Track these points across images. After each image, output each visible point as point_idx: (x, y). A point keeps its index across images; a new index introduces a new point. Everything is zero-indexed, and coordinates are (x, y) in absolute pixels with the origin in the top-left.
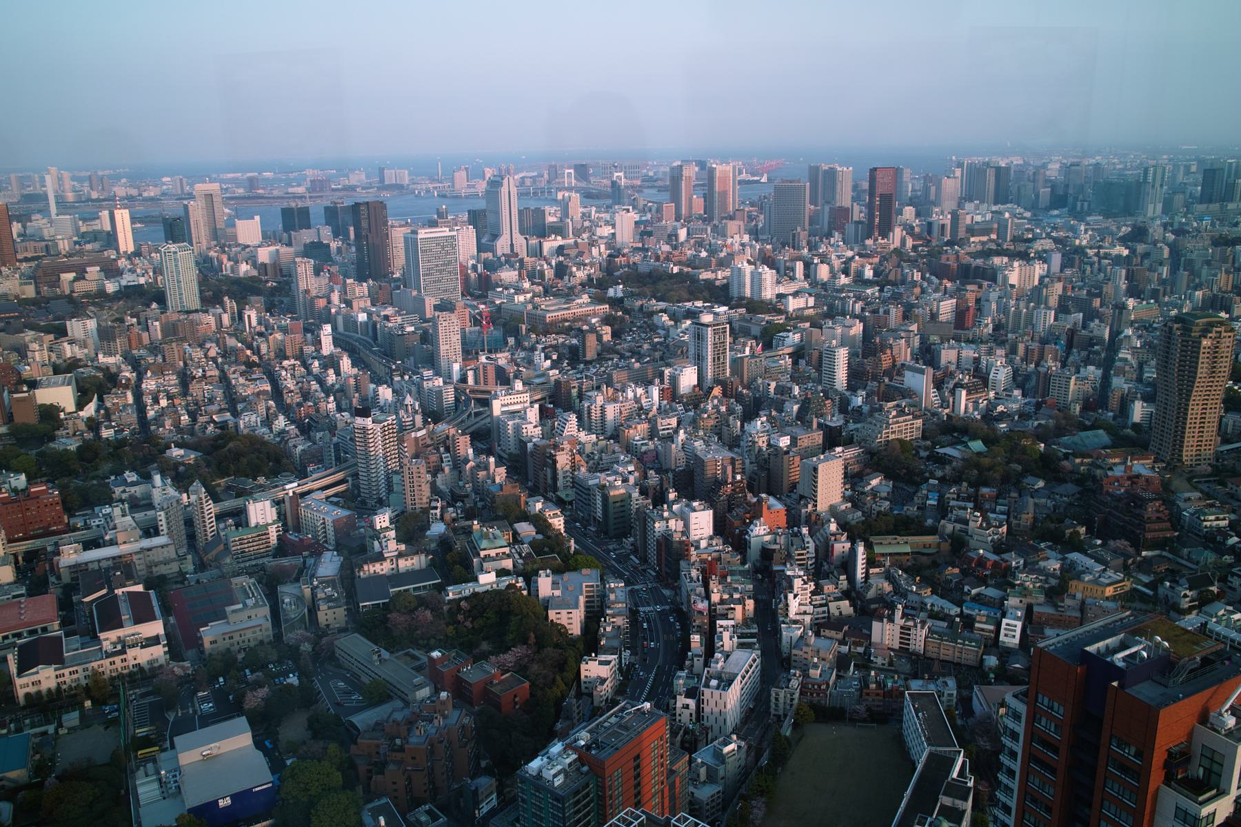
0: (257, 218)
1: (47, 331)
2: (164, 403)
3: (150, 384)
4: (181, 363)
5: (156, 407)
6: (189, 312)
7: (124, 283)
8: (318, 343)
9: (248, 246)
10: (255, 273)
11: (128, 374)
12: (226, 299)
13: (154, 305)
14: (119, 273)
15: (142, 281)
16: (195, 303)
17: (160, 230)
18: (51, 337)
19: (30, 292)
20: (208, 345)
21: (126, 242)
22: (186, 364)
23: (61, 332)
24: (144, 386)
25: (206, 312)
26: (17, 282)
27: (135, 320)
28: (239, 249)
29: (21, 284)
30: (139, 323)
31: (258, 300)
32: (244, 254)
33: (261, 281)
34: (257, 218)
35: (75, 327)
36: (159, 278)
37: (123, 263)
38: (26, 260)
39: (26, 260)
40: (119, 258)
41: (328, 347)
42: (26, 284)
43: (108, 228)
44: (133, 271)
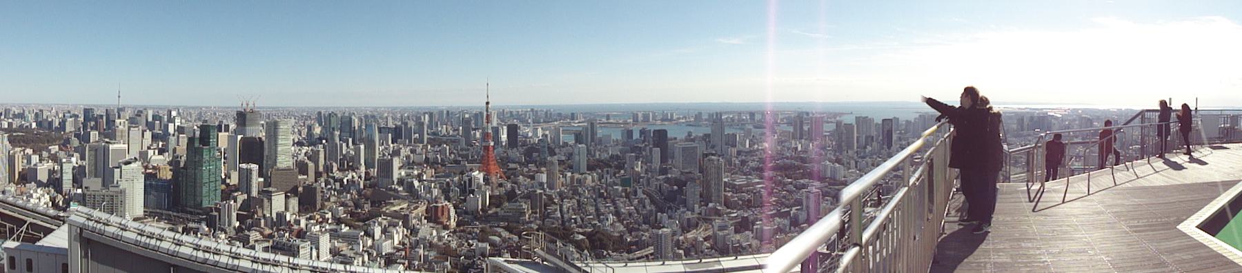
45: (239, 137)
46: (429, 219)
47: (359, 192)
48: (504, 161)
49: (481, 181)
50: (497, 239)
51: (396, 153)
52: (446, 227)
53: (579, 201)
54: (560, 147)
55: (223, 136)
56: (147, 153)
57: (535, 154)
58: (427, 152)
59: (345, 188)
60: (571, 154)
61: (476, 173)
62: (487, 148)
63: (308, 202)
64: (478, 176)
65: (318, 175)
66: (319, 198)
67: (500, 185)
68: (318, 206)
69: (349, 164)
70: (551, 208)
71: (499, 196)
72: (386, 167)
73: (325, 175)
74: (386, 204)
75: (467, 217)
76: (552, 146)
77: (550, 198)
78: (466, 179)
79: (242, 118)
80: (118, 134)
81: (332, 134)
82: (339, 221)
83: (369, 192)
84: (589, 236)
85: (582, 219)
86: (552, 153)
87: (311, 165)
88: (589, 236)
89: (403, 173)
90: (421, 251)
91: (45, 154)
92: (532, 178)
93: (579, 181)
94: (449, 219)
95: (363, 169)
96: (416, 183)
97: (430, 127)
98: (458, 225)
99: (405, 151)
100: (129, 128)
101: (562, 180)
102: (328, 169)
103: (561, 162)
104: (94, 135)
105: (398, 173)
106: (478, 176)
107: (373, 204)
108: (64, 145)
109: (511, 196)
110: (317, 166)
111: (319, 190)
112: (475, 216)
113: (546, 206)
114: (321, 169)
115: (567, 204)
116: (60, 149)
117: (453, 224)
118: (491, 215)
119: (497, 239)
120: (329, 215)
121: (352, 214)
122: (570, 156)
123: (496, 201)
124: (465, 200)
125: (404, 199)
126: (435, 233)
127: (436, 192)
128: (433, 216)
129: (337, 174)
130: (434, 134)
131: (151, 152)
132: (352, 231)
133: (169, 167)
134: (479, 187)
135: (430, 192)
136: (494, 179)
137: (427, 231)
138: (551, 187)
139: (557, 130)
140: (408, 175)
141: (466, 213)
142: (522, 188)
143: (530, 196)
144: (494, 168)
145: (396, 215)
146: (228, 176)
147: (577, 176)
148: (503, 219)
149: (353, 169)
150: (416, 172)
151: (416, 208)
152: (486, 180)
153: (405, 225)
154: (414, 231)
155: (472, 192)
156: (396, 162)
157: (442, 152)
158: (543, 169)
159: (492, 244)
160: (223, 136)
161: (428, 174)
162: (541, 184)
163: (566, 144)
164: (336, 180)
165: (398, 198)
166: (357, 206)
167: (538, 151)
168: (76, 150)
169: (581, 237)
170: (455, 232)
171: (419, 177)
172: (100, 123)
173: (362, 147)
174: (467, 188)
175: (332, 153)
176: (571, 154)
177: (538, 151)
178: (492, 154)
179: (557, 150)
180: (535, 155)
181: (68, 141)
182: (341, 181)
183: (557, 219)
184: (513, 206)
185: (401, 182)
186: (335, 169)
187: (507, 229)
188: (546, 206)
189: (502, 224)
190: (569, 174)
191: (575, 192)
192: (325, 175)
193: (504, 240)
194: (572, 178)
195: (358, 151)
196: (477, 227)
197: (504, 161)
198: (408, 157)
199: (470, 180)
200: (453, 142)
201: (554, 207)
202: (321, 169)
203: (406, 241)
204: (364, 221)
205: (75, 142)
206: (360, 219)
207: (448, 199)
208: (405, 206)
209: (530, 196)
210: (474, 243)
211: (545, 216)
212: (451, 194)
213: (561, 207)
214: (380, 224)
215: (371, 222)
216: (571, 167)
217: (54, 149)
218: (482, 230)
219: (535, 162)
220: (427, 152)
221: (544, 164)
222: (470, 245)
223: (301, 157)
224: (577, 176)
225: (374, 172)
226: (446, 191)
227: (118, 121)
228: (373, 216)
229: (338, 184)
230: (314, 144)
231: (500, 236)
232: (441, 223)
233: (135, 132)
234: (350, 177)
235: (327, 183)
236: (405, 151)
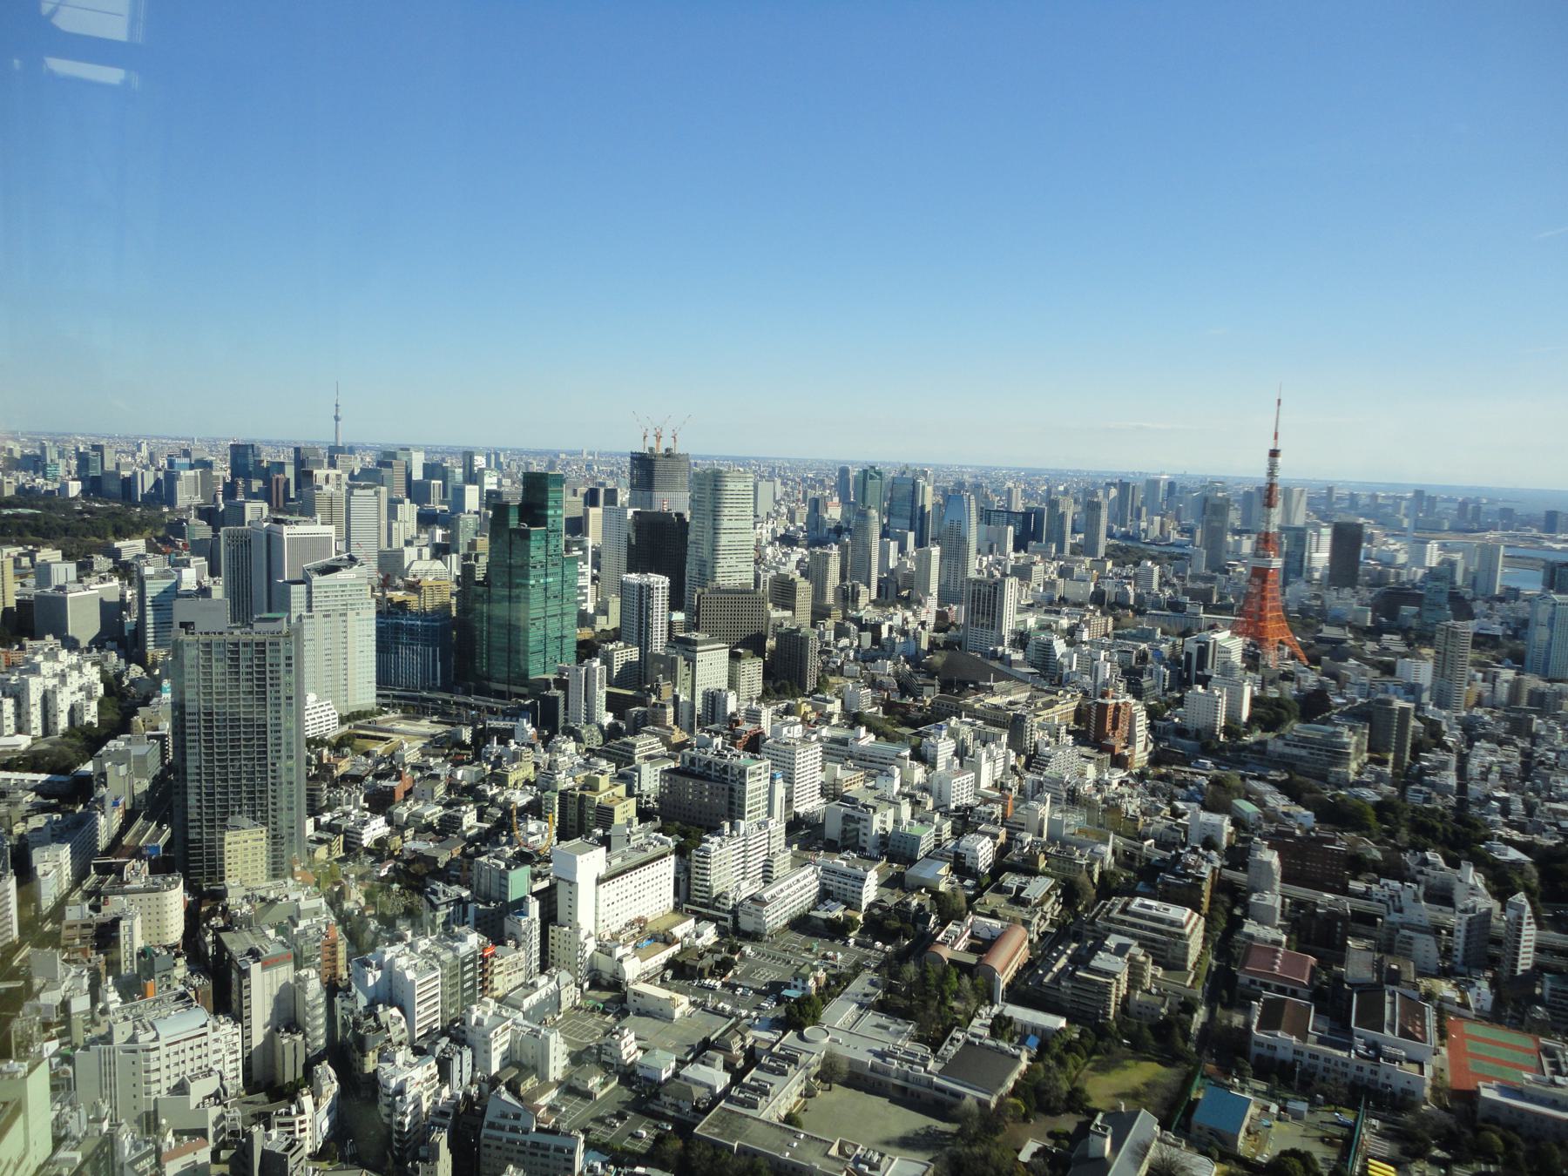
15: (1497, 630)
18: (1377, 673)
22: (1533, 744)
27: (1480, 675)
30: (1484, 680)
40: (1474, 600)
45: (630, 512)
46: (1080, 738)
47: (914, 659)
48: (1305, 619)
49: (1236, 658)
50: (1248, 807)
51: (1023, 573)
52: (1119, 762)
53: (1527, 755)
54: (1492, 599)
55: (595, 513)
56: (399, 555)
57: (1406, 610)
58: (1102, 576)
59: (881, 649)
60: (1525, 623)
61: (1223, 636)
62: (1261, 574)
63: (786, 673)
64: (1230, 643)
65: (820, 613)
66: (814, 664)
67: (1287, 676)
68: (811, 684)
69: (896, 591)
70: (1429, 759)
71: (1278, 703)
72: (986, 600)
73: (837, 615)
74: (978, 689)
75: (1178, 744)
76: (1468, 593)
77: (1434, 729)
78: (1191, 646)
79: (645, 469)
80: (321, 504)
81: (864, 515)
82: (854, 719)
83: (938, 659)
84: (1544, 858)
85: (1530, 809)
86: (1463, 609)
87: (804, 587)
88: (1544, 858)
89: (1031, 621)
90: (1045, 811)
91: (102, 563)
92: (1389, 669)
93: (1538, 699)
94: (1130, 740)
95: (932, 604)
96: (1060, 647)
97: (1118, 517)
98: (1155, 760)
99: (1043, 571)
100: (350, 493)
101: (1480, 686)
102: (848, 597)
103: (1481, 641)
104: (255, 510)
105: (1010, 620)
106: (1230, 643)
107: (946, 687)
108: (168, 538)
109: (1313, 705)
110: (819, 593)
111: (814, 645)
112: (1203, 743)
113: (1417, 748)
114: (830, 599)
115: (1483, 755)
116: (151, 547)
117: (1140, 754)
118: (1245, 748)
119: (1248, 807)
120: (835, 707)
121: (889, 707)
122: (1520, 628)
123: (1268, 714)
124: (1180, 702)
125: (1021, 680)
126: (1091, 772)
127: (1106, 671)
128: (1092, 729)
129: (867, 612)
130: (1126, 536)
131: (410, 553)
132: (885, 747)
133: (455, 588)
134: (1227, 669)
135: (1094, 671)
136: (1271, 658)
137: (1069, 762)
138: (1440, 704)
139: (1489, 553)
140: (1045, 627)
141: (1181, 732)
142: (1351, 692)
143: (1371, 715)
144: (1275, 627)
145: (995, 718)
146: (602, 610)
147: (1532, 682)
148: (1282, 762)
149: (907, 603)
150: (1065, 623)
151: (1049, 705)
152: (1252, 660)
153: (1016, 743)
154: (1034, 760)
155: (1205, 681)
156: (1012, 592)
157: (1142, 579)
158: (1427, 651)
159: (1236, 823)
160: (595, 513)
161: (1098, 625)
162: (1412, 690)
163: (1512, 594)
164: (863, 627)
165: (1008, 677)
166: (905, 688)
167: (1416, 599)
168: (198, 548)
169: (1513, 854)
170: (1141, 777)
171: (1071, 635)
172: (273, 480)
173: (936, 551)
174: (1190, 670)
175: (855, 569)
176: (1525, 623)
177: (1416, 599)
178: (1276, 597)
179: (1479, 607)
180: (1407, 610)
181: (177, 528)
182: (875, 629)
183: (1443, 791)
184: (1314, 731)
185: (1021, 640)
186: (863, 600)
187: (1290, 790)
188: (1417, 748)
189: (1274, 774)
190: (1508, 674)
191: (1520, 727)
192: (837, 615)
193: (1270, 816)
194: (1515, 687)
195: (924, 561)
196: (1205, 772)
197: (1305, 619)
198: (1050, 585)
199: (1203, 652)
200: (1174, 558)
201: (1437, 755)
202: (830, 599)
203: (1013, 782)
204: (914, 724)
205: (202, 530)
206: (907, 719)
207: (1137, 692)
208: (1021, 696)
209: (1371, 715)
210: (1197, 817)
211: (1407, 777)
212: (1146, 682)
213: (1463, 761)
214: (953, 734)
215: (931, 728)
216: (1518, 660)
217: (132, 547)
218: (1216, 782)
219: (1404, 632)
220: (1102, 576)
221: (1425, 638)
222: (1176, 814)
223: (790, 569)
224: (1532, 682)
225: (957, 613)
226: (1132, 677)
227: (320, 473)
228: (937, 715)
229: (867, 637)
230: (822, 543)
231: (1261, 803)
232: (1111, 749)
233: (368, 504)
234: (897, 620)
235: (841, 632)
236: (1043, 571)
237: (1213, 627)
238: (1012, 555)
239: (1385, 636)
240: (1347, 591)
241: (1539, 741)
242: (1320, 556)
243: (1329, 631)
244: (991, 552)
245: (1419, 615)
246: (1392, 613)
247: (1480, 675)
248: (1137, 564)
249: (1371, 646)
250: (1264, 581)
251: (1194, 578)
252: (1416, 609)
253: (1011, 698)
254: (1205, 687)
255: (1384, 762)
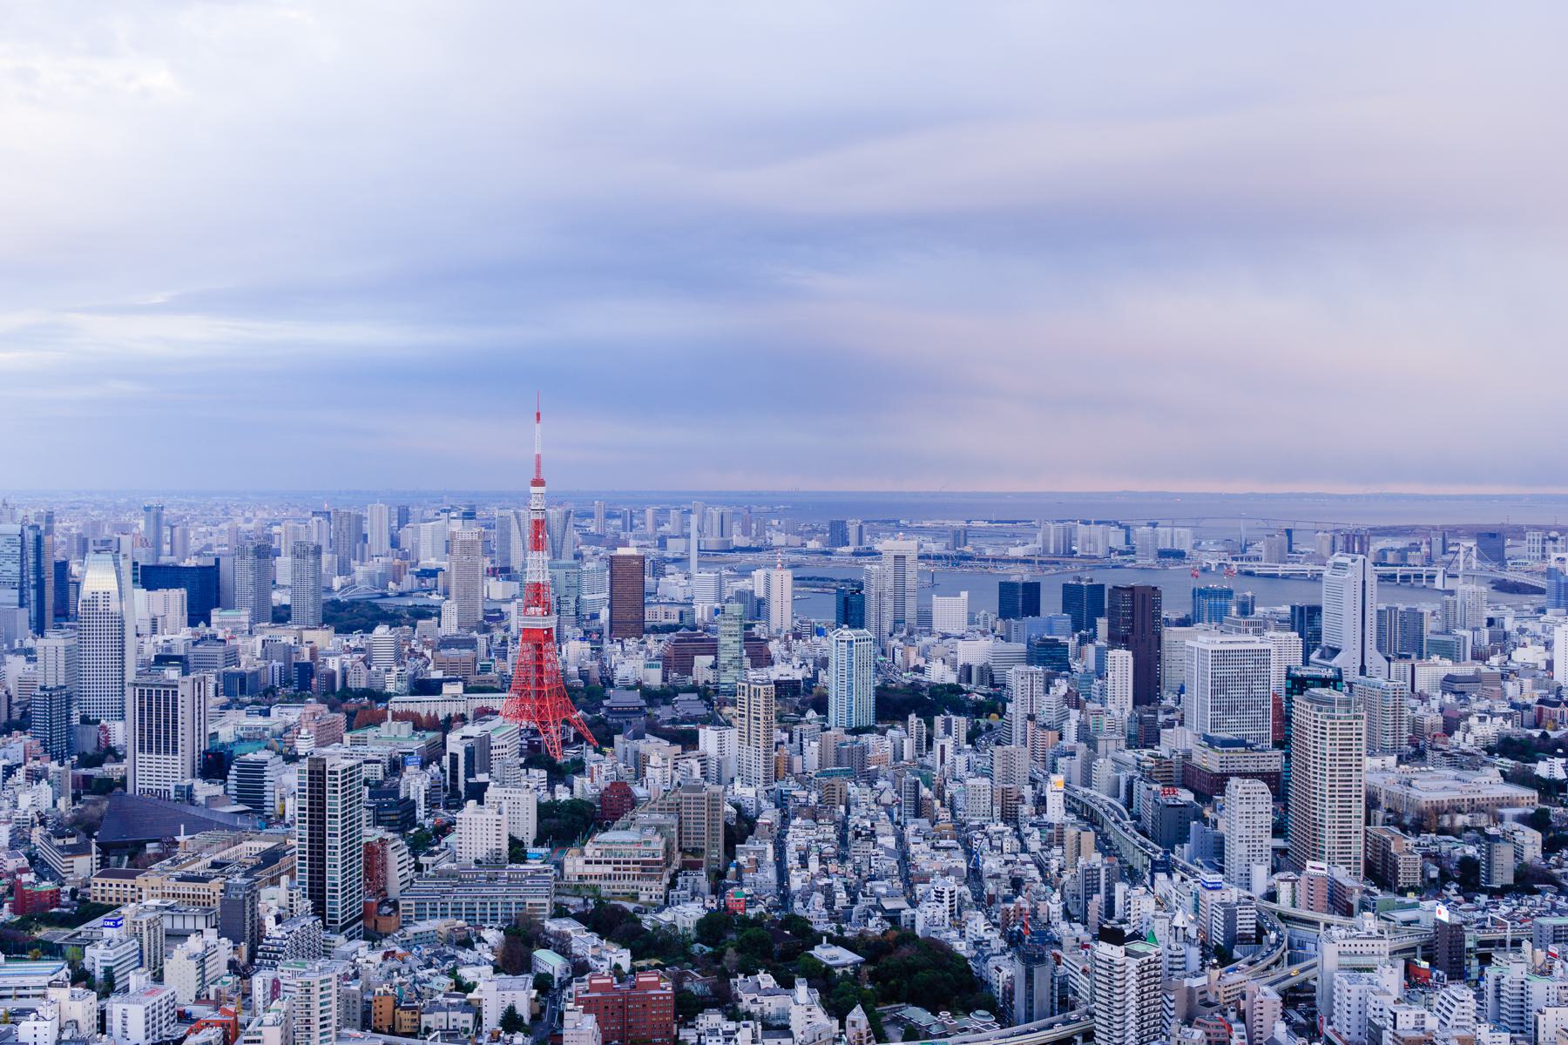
0: (964, 595)
1: (673, 738)
2: (814, 866)
3: (799, 835)
4: (842, 808)
5: (804, 872)
6: (856, 731)
7: (775, 676)
8: (1041, 802)
9: (945, 636)
10: (951, 679)
11: (770, 815)
12: (912, 718)
13: (811, 714)
14: (770, 662)
15: (799, 675)
16: (869, 720)
17: (831, 603)
18: (678, 748)
19: (654, 678)
20: (881, 784)
21: (781, 614)
22: (848, 811)
23: (689, 741)
24: (789, 837)
25: (883, 733)
26: (641, 663)
27: (786, 735)
28: (934, 639)
29: (647, 666)
30: (791, 741)
31: (961, 723)
32: (940, 650)
33: (961, 691)
34: (964, 595)
35: (708, 738)
36: (821, 673)
37: (775, 647)
38: (656, 630)
39: (656, 630)
41: (1055, 811)
42: (651, 666)
43: (760, 593)
44: (788, 661)
53: (842, 827)
107: (105, 849)
155: (478, 792)
185: (214, 764)
237: (483, 714)
238: (186, 633)
239: (682, 696)
240: (631, 643)
241: (852, 807)
242: (597, 598)
243: (617, 698)
244: (154, 631)
245: (714, 667)
246: (687, 669)
247: (786, 735)
248: (369, 630)
249: (663, 713)
250: (539, 647)
251: (447, 643)
252: (709, 659)
253: (217, 857)
254: (481, 802)
255: (696, 866)
